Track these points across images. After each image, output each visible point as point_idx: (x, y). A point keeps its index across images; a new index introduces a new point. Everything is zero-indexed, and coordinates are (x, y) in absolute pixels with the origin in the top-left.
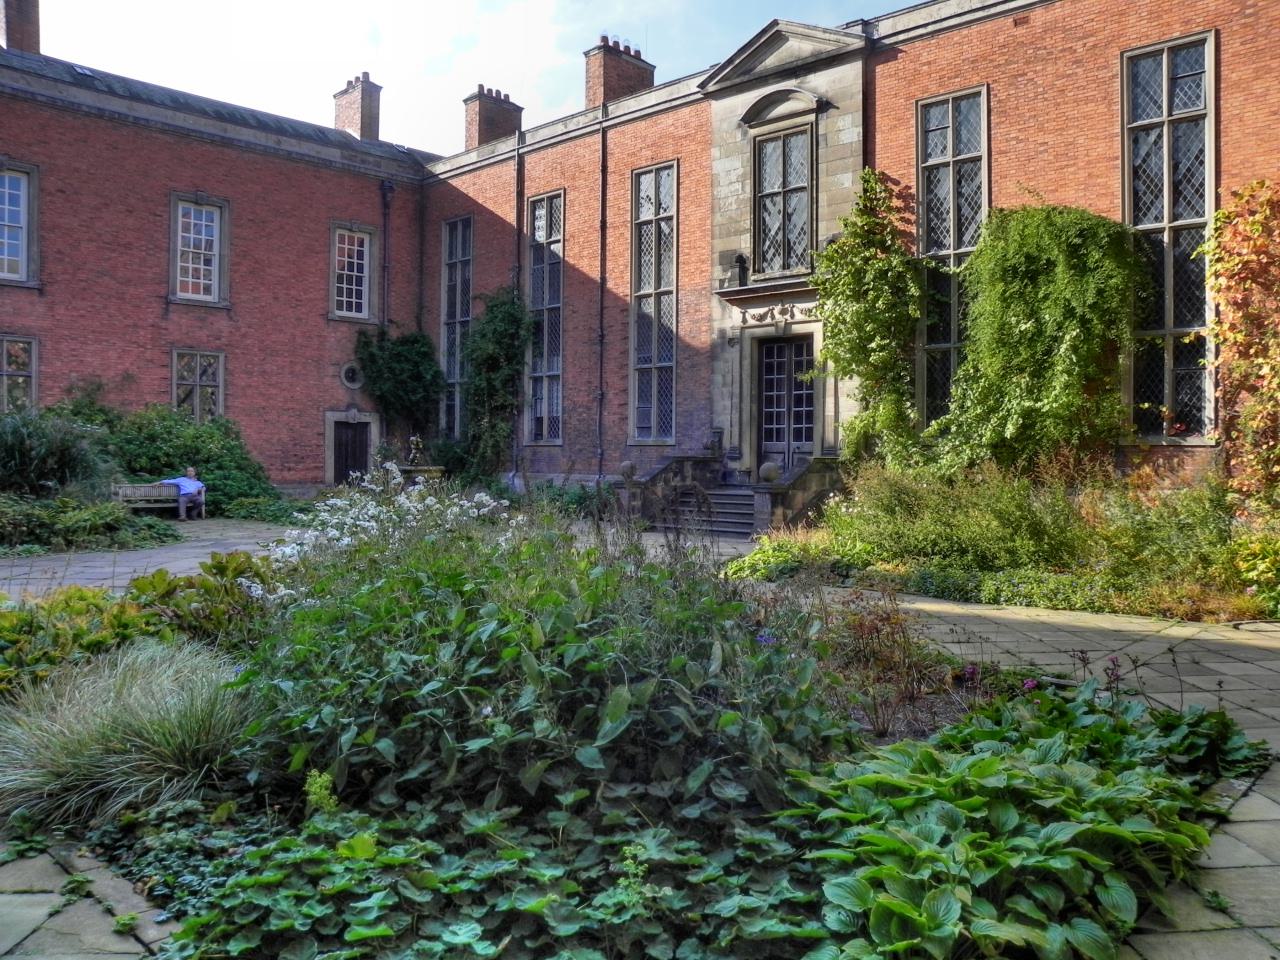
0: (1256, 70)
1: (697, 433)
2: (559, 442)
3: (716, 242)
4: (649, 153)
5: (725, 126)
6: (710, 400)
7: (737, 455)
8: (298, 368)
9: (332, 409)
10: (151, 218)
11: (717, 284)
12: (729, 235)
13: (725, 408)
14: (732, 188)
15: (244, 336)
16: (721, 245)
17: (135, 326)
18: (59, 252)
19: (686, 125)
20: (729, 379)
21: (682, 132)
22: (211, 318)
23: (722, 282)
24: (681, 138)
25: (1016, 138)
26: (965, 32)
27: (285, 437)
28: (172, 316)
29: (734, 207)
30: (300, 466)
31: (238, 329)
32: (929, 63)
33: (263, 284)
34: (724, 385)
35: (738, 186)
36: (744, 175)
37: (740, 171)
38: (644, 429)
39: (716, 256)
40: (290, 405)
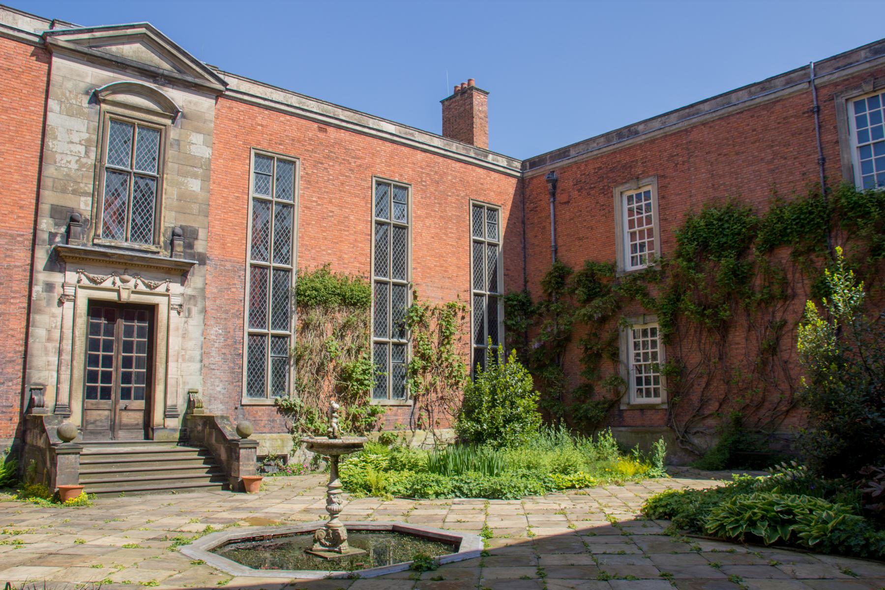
0: (427, 213)
5: (69, 85)
7: (63, 411)
11: (46, 236)
12: (64, 191)
20: (56, 334)
23: (52, 235)
25: (316, 202)
26: (288, 117)
32: (262, 125)
34: (49, 340)
35: (82, 149)
36: (88, 140)
37: (86, 136)
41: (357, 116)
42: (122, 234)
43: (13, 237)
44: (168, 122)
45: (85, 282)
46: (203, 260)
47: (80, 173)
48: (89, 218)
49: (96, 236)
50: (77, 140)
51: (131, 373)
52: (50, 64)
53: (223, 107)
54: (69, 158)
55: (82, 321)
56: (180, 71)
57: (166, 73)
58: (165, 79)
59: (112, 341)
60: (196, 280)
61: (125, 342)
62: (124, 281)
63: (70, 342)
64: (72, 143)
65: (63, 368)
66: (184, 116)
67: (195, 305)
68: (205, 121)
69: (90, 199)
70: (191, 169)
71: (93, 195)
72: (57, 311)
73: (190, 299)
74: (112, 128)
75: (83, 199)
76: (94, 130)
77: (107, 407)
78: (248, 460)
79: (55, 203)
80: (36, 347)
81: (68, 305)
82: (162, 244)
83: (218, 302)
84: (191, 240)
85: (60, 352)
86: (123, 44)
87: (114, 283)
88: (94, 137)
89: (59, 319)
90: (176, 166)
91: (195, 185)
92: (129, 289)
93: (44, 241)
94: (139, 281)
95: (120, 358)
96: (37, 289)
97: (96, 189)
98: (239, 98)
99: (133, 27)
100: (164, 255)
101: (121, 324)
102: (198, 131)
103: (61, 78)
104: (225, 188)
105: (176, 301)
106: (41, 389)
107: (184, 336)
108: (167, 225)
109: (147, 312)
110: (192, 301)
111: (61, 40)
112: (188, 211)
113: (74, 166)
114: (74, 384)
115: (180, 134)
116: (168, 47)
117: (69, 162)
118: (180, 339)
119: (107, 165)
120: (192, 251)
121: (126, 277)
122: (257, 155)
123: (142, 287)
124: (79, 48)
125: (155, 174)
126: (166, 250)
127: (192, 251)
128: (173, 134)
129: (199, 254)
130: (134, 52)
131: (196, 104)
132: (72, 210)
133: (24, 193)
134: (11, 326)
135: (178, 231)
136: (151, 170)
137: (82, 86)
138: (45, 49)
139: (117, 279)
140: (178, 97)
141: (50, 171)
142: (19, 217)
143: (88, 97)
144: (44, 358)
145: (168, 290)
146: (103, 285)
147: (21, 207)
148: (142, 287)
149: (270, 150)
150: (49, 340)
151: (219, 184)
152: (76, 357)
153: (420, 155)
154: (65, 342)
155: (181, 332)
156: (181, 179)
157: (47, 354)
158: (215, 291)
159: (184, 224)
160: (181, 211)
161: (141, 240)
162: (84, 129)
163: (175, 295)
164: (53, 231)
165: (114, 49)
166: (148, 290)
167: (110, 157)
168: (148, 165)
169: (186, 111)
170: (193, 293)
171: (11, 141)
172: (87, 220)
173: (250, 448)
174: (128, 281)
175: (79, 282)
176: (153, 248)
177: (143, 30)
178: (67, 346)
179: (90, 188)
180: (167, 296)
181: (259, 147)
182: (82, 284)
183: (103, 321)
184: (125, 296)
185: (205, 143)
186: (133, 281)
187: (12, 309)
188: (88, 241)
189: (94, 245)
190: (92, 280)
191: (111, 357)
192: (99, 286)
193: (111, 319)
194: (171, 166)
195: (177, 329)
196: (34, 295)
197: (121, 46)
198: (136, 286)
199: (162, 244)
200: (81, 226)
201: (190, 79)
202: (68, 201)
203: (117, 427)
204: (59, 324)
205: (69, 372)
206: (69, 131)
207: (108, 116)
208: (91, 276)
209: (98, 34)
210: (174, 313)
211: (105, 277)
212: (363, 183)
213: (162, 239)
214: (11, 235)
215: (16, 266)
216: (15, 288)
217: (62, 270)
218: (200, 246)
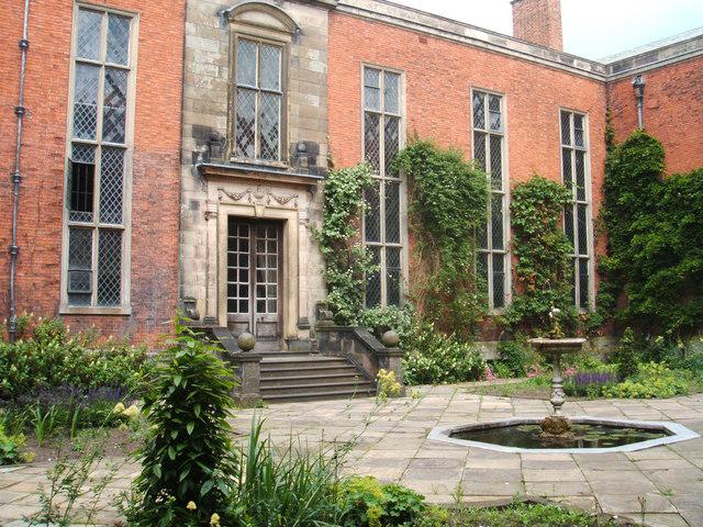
5: (202, 7)
11: (190, 156)
16: (192, 118)
20: (203, 250)
23: (195, 155)
29: (211, 87)
36: (221, 61)
37: (218, 56)
38: (79, 294)
39: (188, 128)
41: (453, 26)
44: (288, 38)
45: (226, 199)
50: (211, 61)
54: (205, 79)
55: (224, 236)
64: (207, 63)
65: (210, 283)
66: (301, 33)
69: (225, 118)
71: (228, 114)
80: (187, 262)
81: (212, 222)
85: (207, 267)
89: (204, 236)
91: (315, 101)
93: (188, 161)
96: (186, 206)
102: (314, 47)
106: (193, 304)
117: (206, 82)
122: (365, 67)
123: (274, 203)
128: (294, 51)
132: (210, 130)
133: (168, 114)
135: (301, 147)
137: (214, 8)
141: (191, 92)
148: (274, 203)
149: (378, 64)
150: (197, 255)
153: (512, 63)
154: (210, 257)
157: (196, 270)
160: (303, 127)
162: (217, 50)
164: (195, 150)
171: (156, 64)
176: (281, 165)
178: (213, 262)
181: (367, 61)
185: (321, 59)
189: (234, 163)
194: (293, 83)
198: (268, 202)
204: (205, 240)
206: (205, 52)
207: (237, 35)
212: (463, 94)
216: (166, 207)
218: (321, 162)
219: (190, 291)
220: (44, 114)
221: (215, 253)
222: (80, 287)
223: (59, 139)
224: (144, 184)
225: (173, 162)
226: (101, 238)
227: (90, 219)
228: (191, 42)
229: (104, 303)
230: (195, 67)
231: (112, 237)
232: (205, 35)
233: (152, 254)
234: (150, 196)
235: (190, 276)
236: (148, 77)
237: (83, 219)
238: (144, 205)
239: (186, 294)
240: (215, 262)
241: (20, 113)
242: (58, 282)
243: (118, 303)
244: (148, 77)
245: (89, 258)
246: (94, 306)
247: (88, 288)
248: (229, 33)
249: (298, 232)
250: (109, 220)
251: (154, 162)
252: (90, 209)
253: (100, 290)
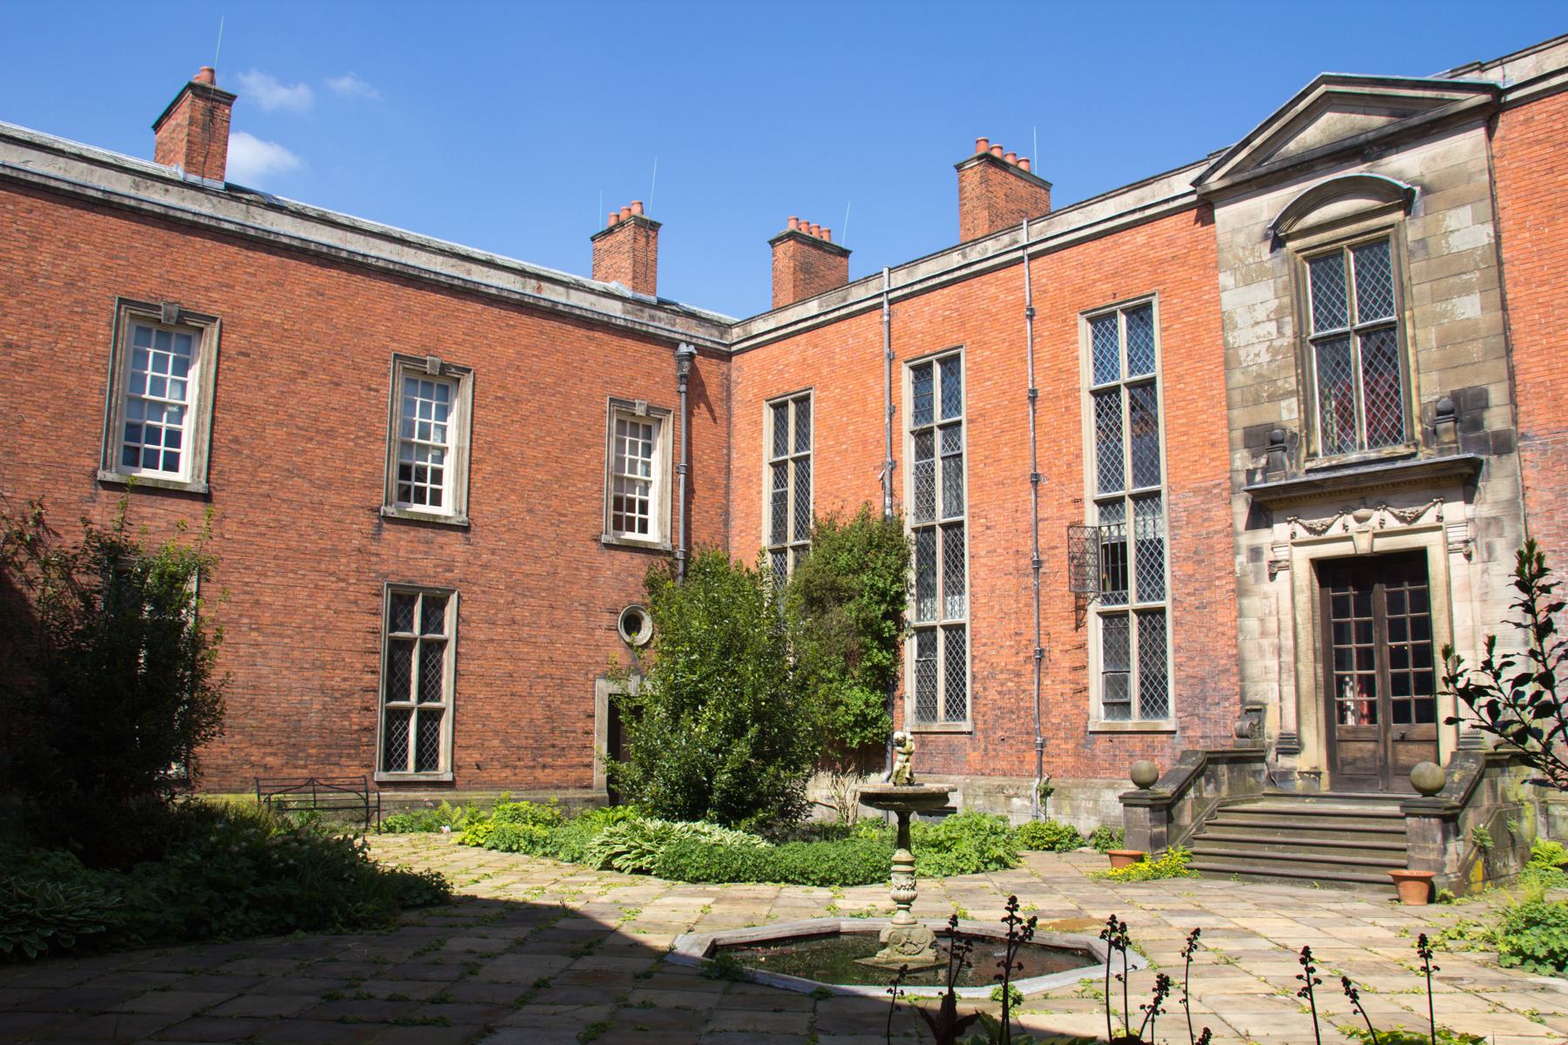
1: (1216, 712)
2: (966, 726)
3: (1235, 413)
4: (1107, 287)
5: (1241, 239)
6: (1239, 661)
7: (1291, 745)
8: (559, 614)
9: (605, 676)
10: (363, 393)
11: (1242, 478)
13: (1266, 670)
14: (1260, 330)
15: (484, 566)
16: (1244, 418)
17: (334, 549)
18: (236, 440)
19: (1171, 242)
20: (1272, 625)
21: (1167, 253)
22: (440, 539)
23: (1251, 474)
24: (1162, 262)
27: (539, 713)
28: (385, 535)
30: (560, 762)
31: (477, 556)
33: (513, 490)
34: (1264, 634)
35: (1272, 327)
37: (1274, 304)
38: (1117, 706)
39: (1238, 434)
40: (547, 670)
42: (1353, 440)
43: (1208, 491)
44: (1398, 216)
45: (1302, 534)
46: (1503, 444)
47: (1274, 365)
48: (1296, 430)
49: (1312, 456)
51: (1406, 675)
52: (1213, 221)
53: (1511, 129)
54: (1256, 349)
56: (1404, 116)
57: (1371, 136)
58: (1379, 146)
59: (1369, 623)
60: (1496, 487)
61: (1390, 621)
62: (1359, 520)
63: (1290, 634)
64: (1257, 323)
65: (1284, 676)
66: (1426, 190)
67: (1500, 535)
68: (1469, 177)
69: (1294, 400)
70: (1456, 279)
72: (1267, 586)
73: (1489, 524)
74: (1313, 272)
75: (1284, 404)
76: (1285, 289)
77: (1370, 736)
78: (1425, 839)
79: (1247, 424)
80: (1249, 648)
81: (1283, 576)
82: (1418, 436)
83: (1558, 519)
84: (1476, 413)
85: (1279, 651)
86: (1304, 128)
87: (1345, 527)
88: (1286, 300)
89: (1273, 600)
90: (1427, 286)
91: (1470, 308)
92: (1362, 532)
94: (1386, 515)
95: (1386, 651)
96: (1242, 558)
97: (1304, 381)
98: (1541, 90)
99: (1304, 95)
100: (1425, 456)
101: (1381, 593)
102: (1457, 204)
103: (1229, 236)
104: (1543, 283)
105: (1457, 535)
107: (1484, 599)
108: (1425, 400)
109: (1413, 564)
110: (1493, 529)
111: (1214, 182)
112: (1463, 361)
113: (1265, 358)
114: (1303, 700)
115: (1425, 227)
116: (1367, 90)
117: (1257, 355)
118: (1477, 605)
119: (1313, 335)
120: (1481, 433)
121: (1362, 512)
123: (1393, 524)
124: (1238, 178)
125: (1394, 318)
126: (1427, 446)
127: (1481, 433)
128: (1412, 232)
129: (1497, 435)
130: (1323, 131)
131: (1445, 157)
132: (1271, 427)
133: (1213, 423)
134: (1220, 620)
136: (1386, 313)
137: (1258, 230)
138: (1205, 206)
139: (1349, 519)
140: (1404, 165)
142: (1212, 460)
143: (1269, 243)
144: (1260, 663)
145: (1440, 518)
146: (1330, 533)
147: (1213, 445)
148: (1393, 524)
150: (1264, 634)
151: (1527, 282)
152: (1302, 656)
155: (1476, 591)
156: (1440, 307)
157: (1262, 656)
158: (1551, 497)
159: (1456, 388)
160: (1448, 366)
161: (1386, 442)
162: (1271, 295)
163: (1455, 525)
164: (1251, 467)
165: (1292, 147)
166: (1404, 526)
167: (1317, 321)
168: (1380, 307)
169: (1427, 180)
170: (1493, 513)
171: (1189, 356)
172: (1294, 435)
173: (1425, 816)
174: (1366, 519)
175: (1293, 535)
176: (1401, 450)
177: (1323, 89)
179: (1292, 383)
180: (1444, 530)
182: (1297, 539)
183: (1351, 592)
184: (1363, 545)
185: (1477, 220)
186: (1376, 516)
187: (1220, 595)
188: (1298, 467)
190: (1311, 530)
191: (1369, 651)
192: (1323, 537)
193: (1365, 588)
195: (1469, 586)
196: (1237, 569)
197: (1302, 135)
198: (1382, 523)
199: (1418, 436)
200: (1284, 449)
201: (1415, 121)
202: (1263, 415)
203: (1391, 772)
204: (1274, 607)
205: (1292, 681)
208: (1307, 523)
209: (1257, 142)
210: (1457, 559)
211: (1328, 520)
213: (1418, 428)
214: (1206, 489)
215: (1216, 532)
217: (1269, 526)
218: (1496, 420)
219: (1256, 692)
220: (1061, 474)
221: (1290, 624)
222: (1116, 694)
223: (1078, 501)
224: (1186, 534)
225: (1225, 494)
226: (1141, 623)
227: (1125, 600)
228: (1228, 301)
229: (1147, 715)
230: (1238, 338)
231: (1153, 618)
232: (1248, 282)
233: (1202, 638)
234: (1195, 553)
235: (1253, 669)
236: (1180, 378)
237: (1117, 601)
238: (1189, 568)
239: (1250, 697)
240: (1290, 643)
241: (1036, 480)
242: (1086, 689)
243: (1165, 714)
244: (1180, 378)
245: (1127, 653)
246: (1134, 721)
247: (1126, 694)
248: (1285, 260)
249: (1448, 569)
250: (1149, 596)
251: (1197, 500)
252: (1125, 587)
253: (1143, 696)
